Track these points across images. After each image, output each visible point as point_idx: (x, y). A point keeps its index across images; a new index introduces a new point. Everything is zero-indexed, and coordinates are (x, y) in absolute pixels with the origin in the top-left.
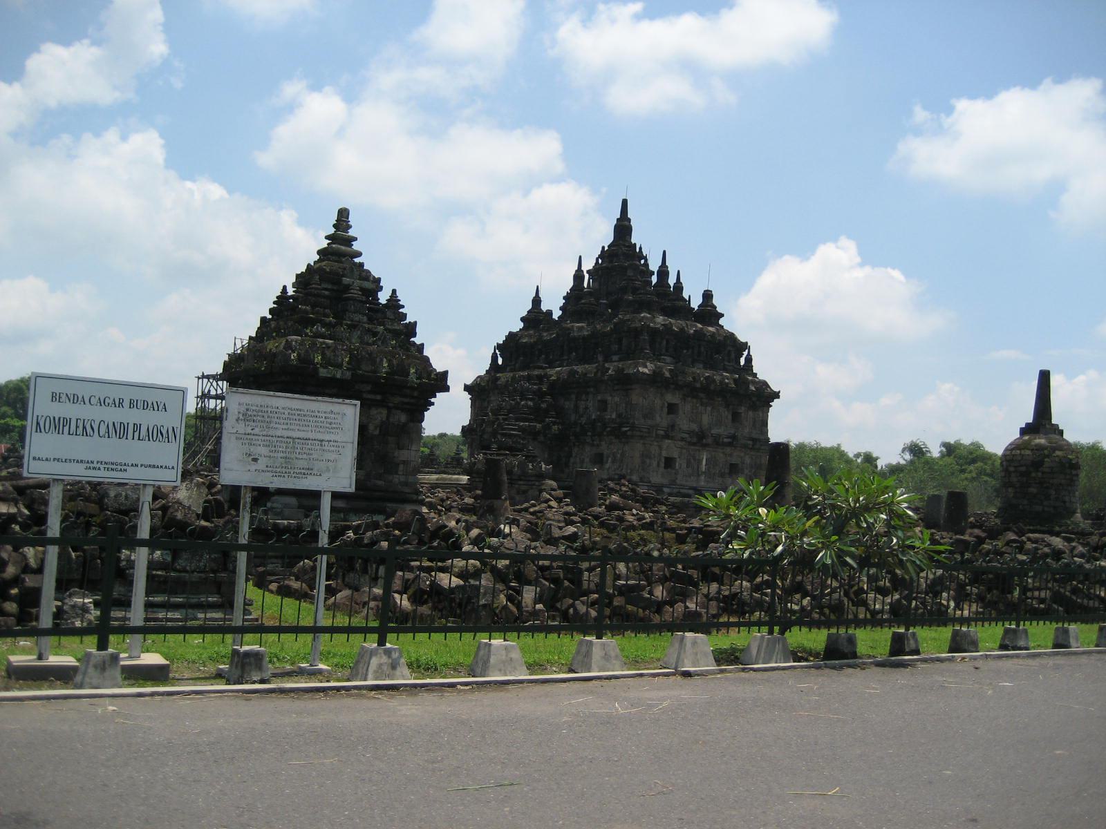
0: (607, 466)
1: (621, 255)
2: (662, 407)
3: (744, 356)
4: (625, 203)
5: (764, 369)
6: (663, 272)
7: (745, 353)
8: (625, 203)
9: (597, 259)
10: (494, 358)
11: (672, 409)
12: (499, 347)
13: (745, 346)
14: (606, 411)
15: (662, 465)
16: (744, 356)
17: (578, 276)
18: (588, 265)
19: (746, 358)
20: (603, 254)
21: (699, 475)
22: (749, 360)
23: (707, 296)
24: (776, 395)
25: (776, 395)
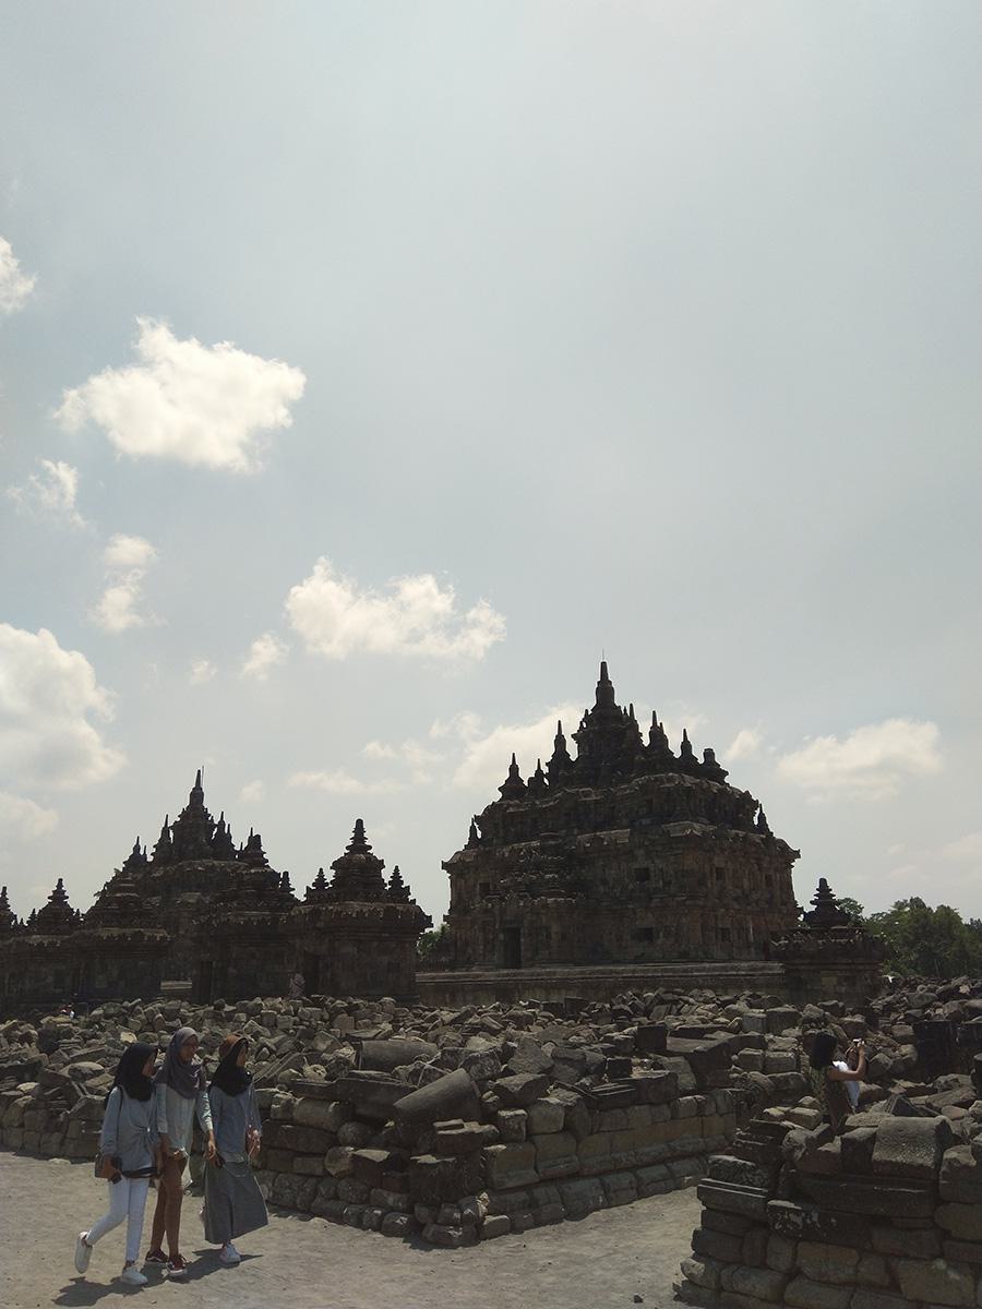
0: (659, 942)
1: (607, 721)
2: (711, 873)
3: (757, 815)
4: (604, 665)
5: (778, 829)
6: (657, 733)
7: (758, 812)
8: (604, 665)
9: (581, 723)
10: (473, 830)
11: (720, 873)
12: (476, 819)
13: (756, 804)
14: (648, 879)
15: (720, 937)
16: (757, 815)
17: (560, 741)
18: (572, 727)
19: (759, 818)
20: (587, 718)
21: (749, 947)
22: (762, 817)
23: (709, 754)
24: (797, 854)
25: (797, 854)
